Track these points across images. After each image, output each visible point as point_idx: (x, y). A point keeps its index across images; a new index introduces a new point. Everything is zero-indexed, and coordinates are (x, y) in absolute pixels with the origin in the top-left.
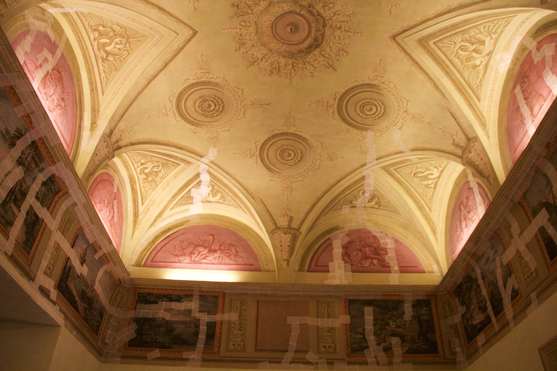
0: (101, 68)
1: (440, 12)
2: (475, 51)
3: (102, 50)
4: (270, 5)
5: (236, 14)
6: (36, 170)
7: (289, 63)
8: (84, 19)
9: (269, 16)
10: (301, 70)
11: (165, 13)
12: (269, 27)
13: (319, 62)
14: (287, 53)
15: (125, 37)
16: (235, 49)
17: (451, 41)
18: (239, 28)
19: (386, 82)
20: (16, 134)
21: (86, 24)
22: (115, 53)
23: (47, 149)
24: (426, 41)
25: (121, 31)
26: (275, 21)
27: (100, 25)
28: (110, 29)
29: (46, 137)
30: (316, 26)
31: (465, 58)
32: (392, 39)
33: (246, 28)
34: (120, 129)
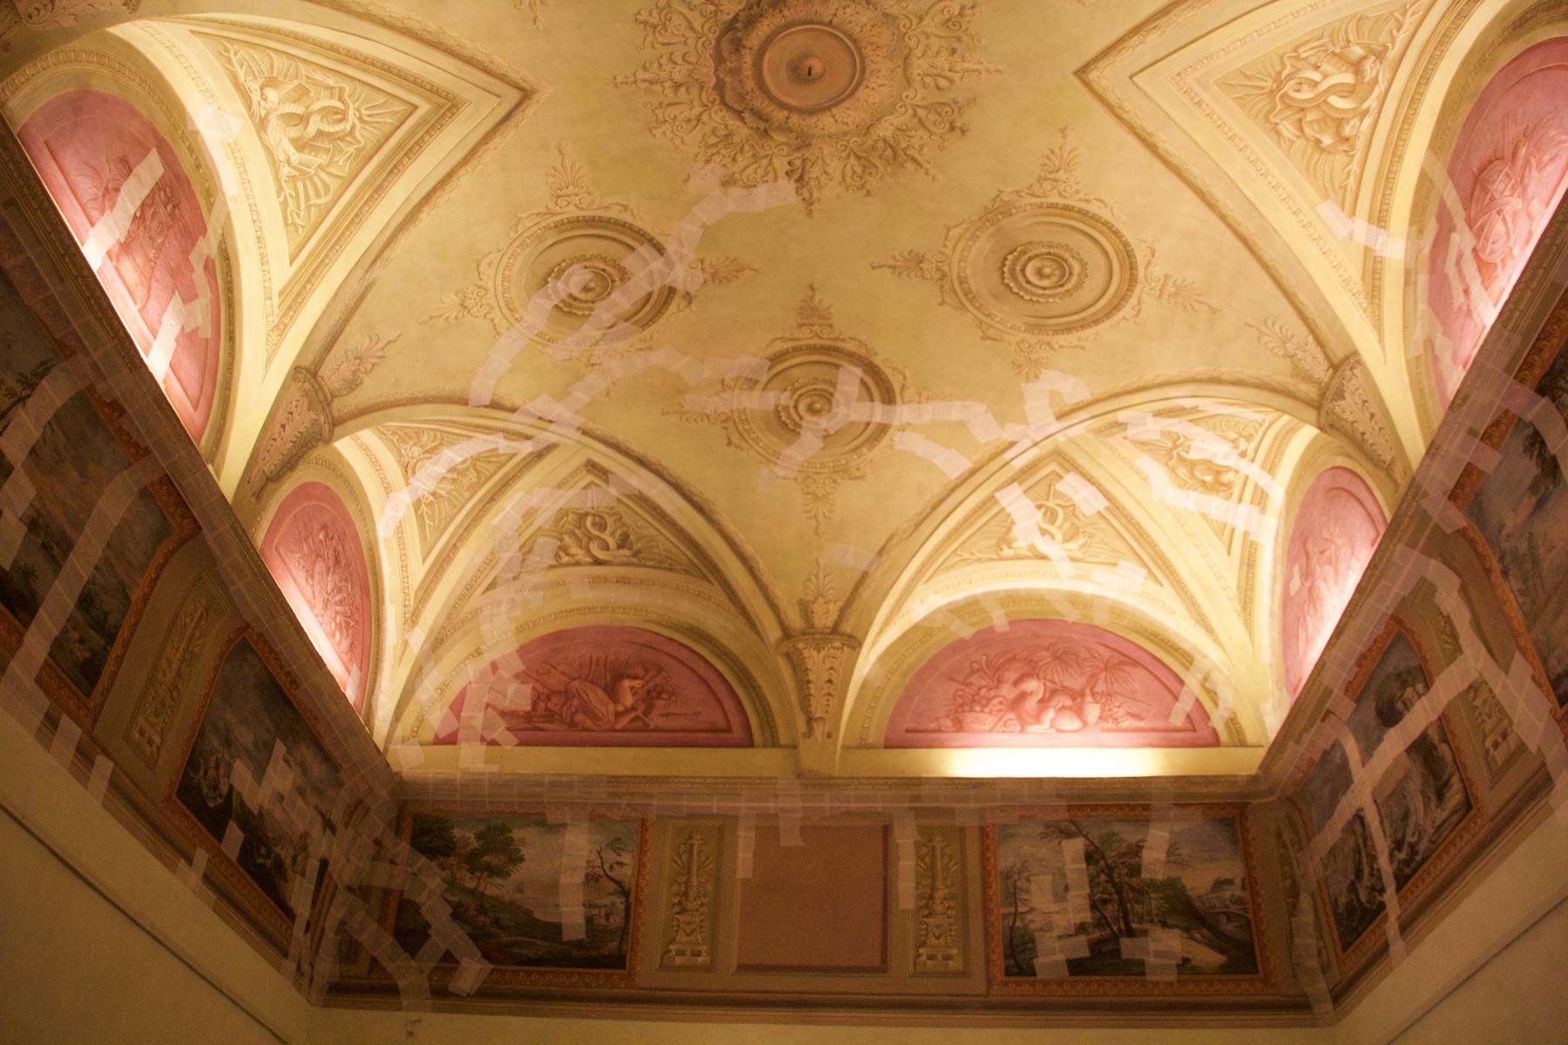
0: (1401, 38)
1: (448, 188)
2: (303, 119)
4: (868, 128)
5: (960, 109)
8: (1351, 182)
9: (870, 100)
12: (872, 72)
15: (1282, 97)
16: (978, 9)
17: (377, 122)
18: (956, 72)
20: (1536, 452)
21: (1355, 166)
22: (1334, 61)
24: (440, 106)
25: (1282, 116)
28: (1308, 130)
29: (1508, 370)
30: (741, 82)
31: (312, 94)
32: (528, 88)
33: (935, 72)
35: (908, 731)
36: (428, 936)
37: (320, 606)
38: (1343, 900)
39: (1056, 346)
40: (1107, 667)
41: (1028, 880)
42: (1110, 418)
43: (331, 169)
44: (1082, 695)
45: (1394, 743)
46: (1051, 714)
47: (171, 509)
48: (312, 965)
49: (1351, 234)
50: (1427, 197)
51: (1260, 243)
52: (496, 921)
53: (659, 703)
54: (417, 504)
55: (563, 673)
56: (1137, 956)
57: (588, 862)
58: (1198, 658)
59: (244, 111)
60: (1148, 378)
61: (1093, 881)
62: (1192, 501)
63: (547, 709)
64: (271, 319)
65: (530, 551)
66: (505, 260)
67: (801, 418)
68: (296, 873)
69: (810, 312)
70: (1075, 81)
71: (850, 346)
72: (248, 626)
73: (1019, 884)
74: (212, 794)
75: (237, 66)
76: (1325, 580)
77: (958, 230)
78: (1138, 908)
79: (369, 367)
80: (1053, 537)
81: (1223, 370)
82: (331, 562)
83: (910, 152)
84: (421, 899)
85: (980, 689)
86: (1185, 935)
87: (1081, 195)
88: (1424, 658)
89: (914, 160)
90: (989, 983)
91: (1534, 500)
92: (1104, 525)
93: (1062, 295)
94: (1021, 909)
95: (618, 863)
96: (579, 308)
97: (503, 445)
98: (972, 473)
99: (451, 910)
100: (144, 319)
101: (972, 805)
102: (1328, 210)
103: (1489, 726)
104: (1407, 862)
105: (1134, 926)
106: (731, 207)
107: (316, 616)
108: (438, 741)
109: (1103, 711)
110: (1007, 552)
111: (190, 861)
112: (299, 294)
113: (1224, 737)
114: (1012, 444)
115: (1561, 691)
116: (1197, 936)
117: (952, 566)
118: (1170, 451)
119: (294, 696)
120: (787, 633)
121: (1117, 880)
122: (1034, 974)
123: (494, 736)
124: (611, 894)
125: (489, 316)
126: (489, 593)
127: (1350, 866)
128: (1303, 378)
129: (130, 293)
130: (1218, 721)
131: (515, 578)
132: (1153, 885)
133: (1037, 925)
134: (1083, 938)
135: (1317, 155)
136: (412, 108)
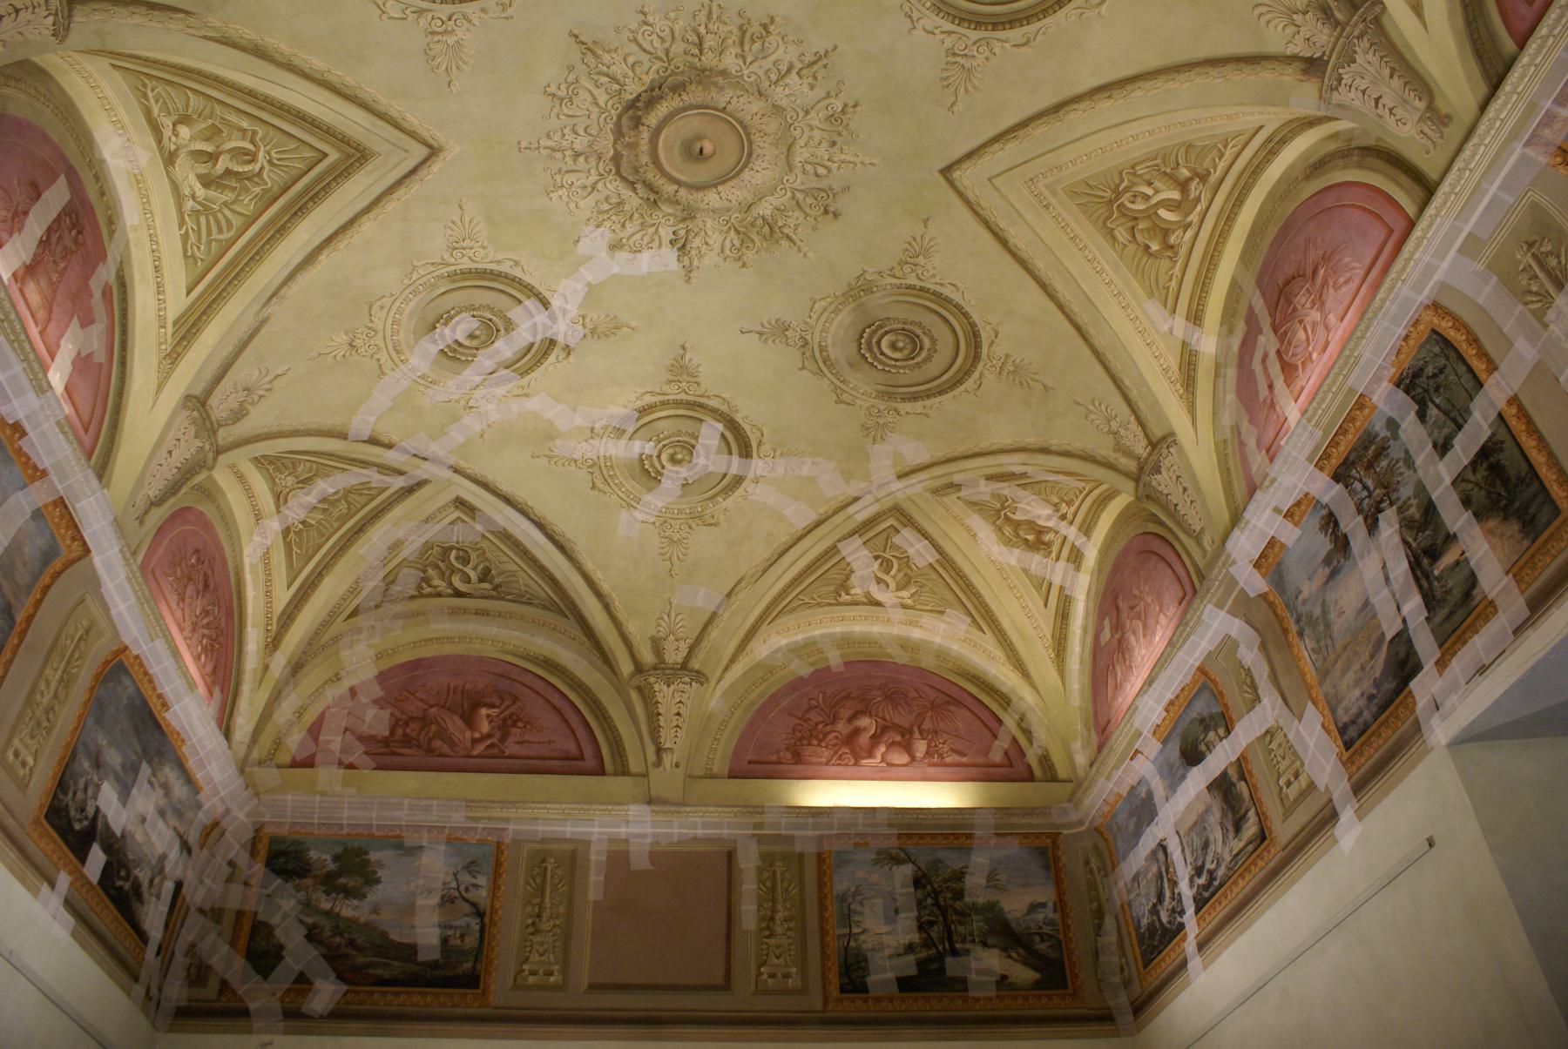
0: (1222, 165)
1: (349, 233)
2: (212, 157)
3: (1192, 196)
5: (834, 195)
6: (1395, 452)
7: (710, 55)
8: (1173, 284)
9: (753, 181)
10: (677, 34)
11: (997, 230)
13: (625, 60)
14: (715, 84)
16: (858, 108)
19: (411, 17)
21: (1177, 271)
22: (1166, 178)
23: (1337, 439)
24: (349, 156)
26: (742, 170)
27: (1151, 255)
28: (1139, 237)
29: (1310, 459)
34: (1290, 30)
35: (750, 762)
36: (282, 958)
37: (188, 628)
38: (1145, 922)
39: (903, 413)
40: (933, 706)
41: (861, 903)
42: (946, 480)
43: (234, 207)
44: (911, 732)
45: (1197, 780)
46: (882, 749)
47: (63, 531)
48: (160, 989)
49: (1171, 330)
50: (1237, 302)
51: (1092, 332)
52: (352, 943)
53: (514, 730)
54: (286, 532)
55: (421, 700)
56: (961, 974)
57: (444, 884)
58: (1014, 699)
59: (154, 144)
60: (984, 445)
61: (920, 904)
62: (1013, 558)
63: (405, 734)
64: (163, 347)
65: (392, 582)
66: (397, 304)
67: (663, 467)
68: (151, 895)
69: (680, 369)
70: (941, 179)
71: (714, 403)
72: (126, 648)
73: (852, 907)
74: (78, 816)
75: (153, 102)
76: (1134, 633)
77: (824, 303)
78: (961, 929)
79: (256, 398)
80: (887, 586)
81: (1052, 442)
82: (201, 587)
83: (786, 230)
84: (275, 920)
85: (817, 724)
86: (1003, 954)
87: (937, 280)
88: (1226, 705)
89: (789, 238)
90: (826, 1001)
91: (1328, 571)
92: (935, 576)
93: (912, 368)
94: (855, 930)
95: (473, 885)
96: (463, 354)
97: (375, 478)
98: (818, 524)
99: (306, 932)
100: (44, 341)
101: (810, 833)
102: (1153, 308)
103: (1283, 766)
104: (1206, 887)
105: (958, 946)
106: (616, 269)
107: (185, 638)
108: (295, 764)
109: (929, 746)
110: (845, 598)
111: (52, 885)
112: (194, 325)
113: (1037, 772)
114: (856, 499)
115: (1346, 737)
116: (1014, 955)
117: (795, 609)
118: (998, 512)
119: (164, 718)
120: (639, 668)
121: (942, 903)
122: (867, 992)
123: (351, 759)
124: (466, 915)
125: (376, 356)
126: (350, 621)
127: (1153, 891)
128: (1125, 453)
129: (33, 315)
130: (1032, 758)
131: (377, 607)
132: (974, 908)
133: (870, 945)
134: (911, 958)
135: (1145, 259)
136: (321, 156)
